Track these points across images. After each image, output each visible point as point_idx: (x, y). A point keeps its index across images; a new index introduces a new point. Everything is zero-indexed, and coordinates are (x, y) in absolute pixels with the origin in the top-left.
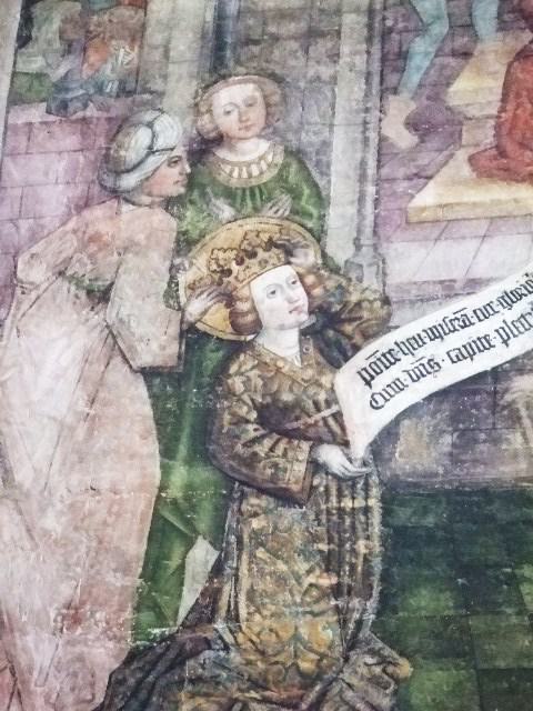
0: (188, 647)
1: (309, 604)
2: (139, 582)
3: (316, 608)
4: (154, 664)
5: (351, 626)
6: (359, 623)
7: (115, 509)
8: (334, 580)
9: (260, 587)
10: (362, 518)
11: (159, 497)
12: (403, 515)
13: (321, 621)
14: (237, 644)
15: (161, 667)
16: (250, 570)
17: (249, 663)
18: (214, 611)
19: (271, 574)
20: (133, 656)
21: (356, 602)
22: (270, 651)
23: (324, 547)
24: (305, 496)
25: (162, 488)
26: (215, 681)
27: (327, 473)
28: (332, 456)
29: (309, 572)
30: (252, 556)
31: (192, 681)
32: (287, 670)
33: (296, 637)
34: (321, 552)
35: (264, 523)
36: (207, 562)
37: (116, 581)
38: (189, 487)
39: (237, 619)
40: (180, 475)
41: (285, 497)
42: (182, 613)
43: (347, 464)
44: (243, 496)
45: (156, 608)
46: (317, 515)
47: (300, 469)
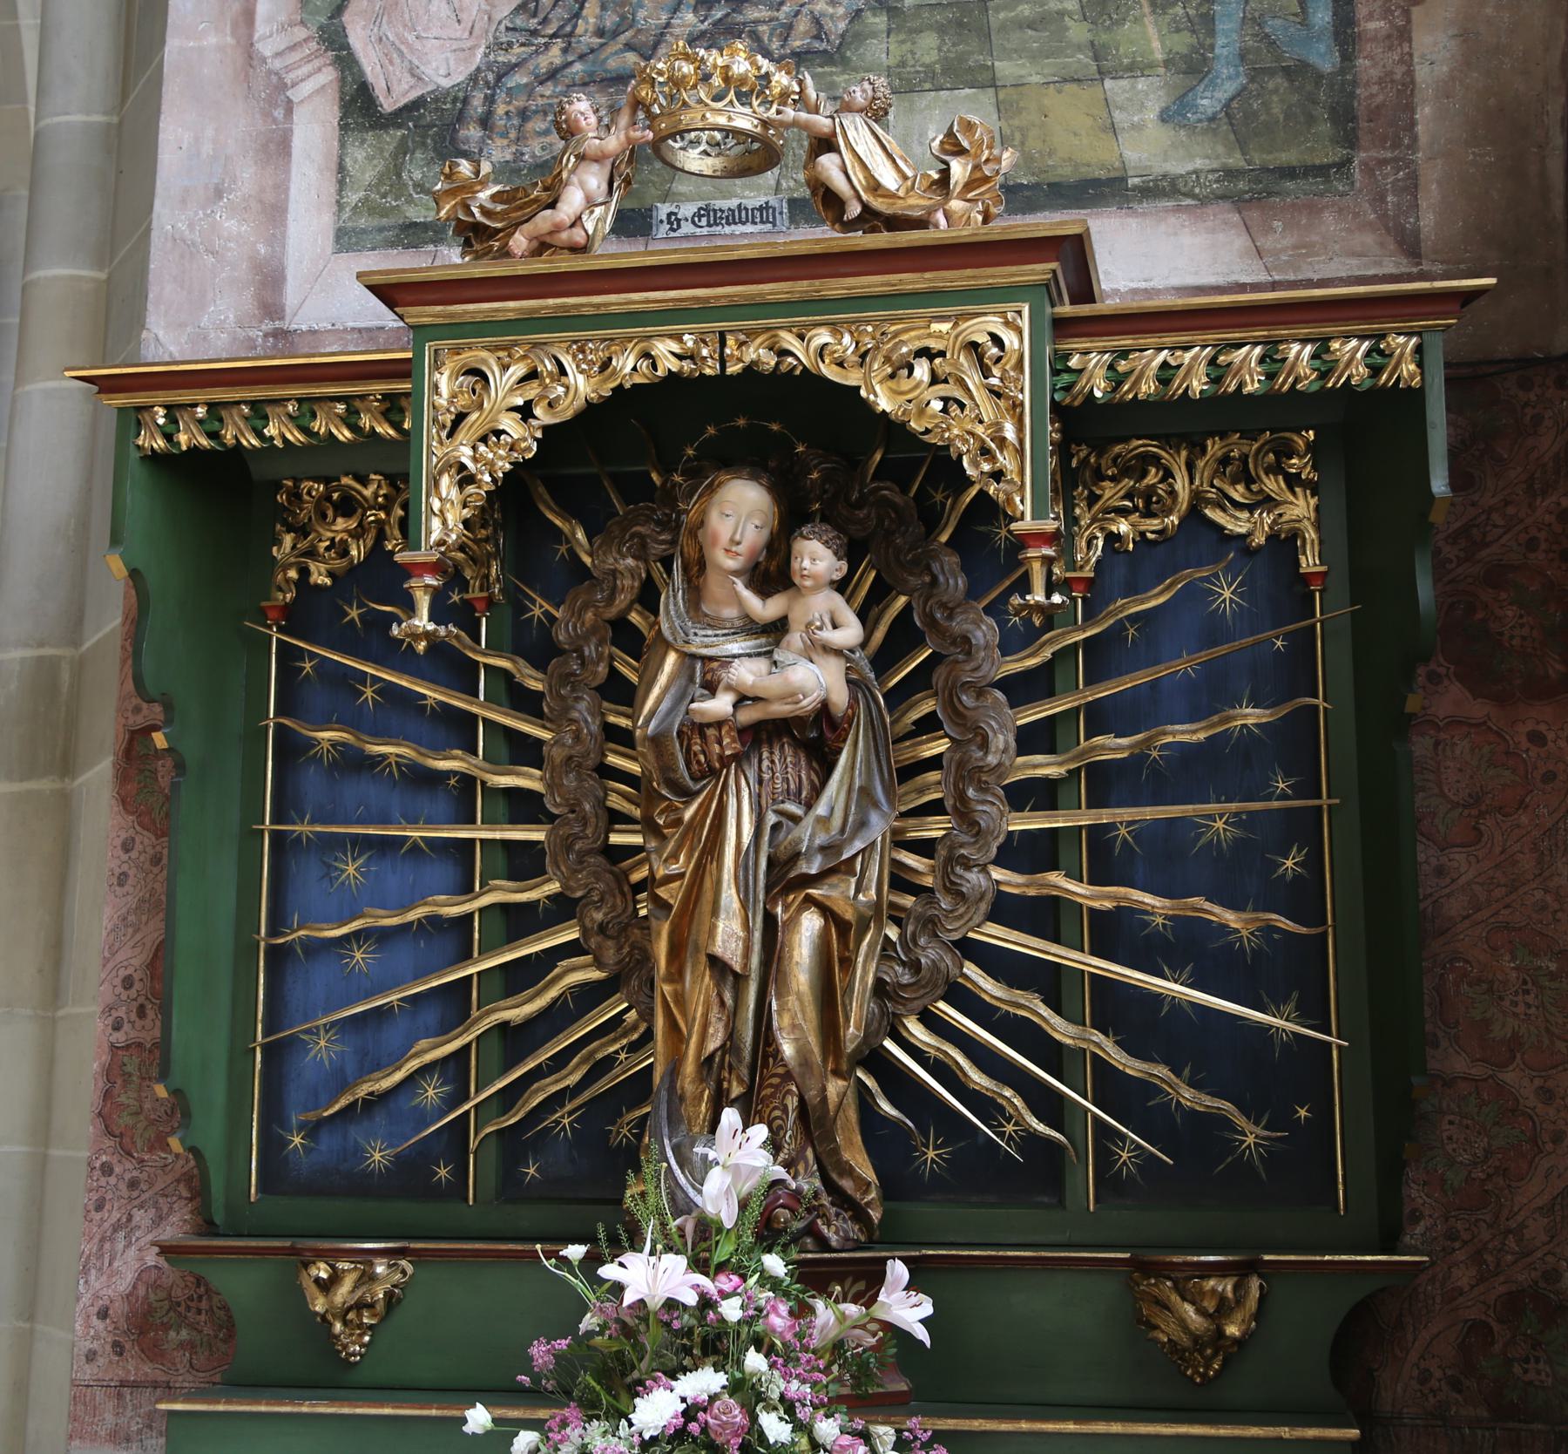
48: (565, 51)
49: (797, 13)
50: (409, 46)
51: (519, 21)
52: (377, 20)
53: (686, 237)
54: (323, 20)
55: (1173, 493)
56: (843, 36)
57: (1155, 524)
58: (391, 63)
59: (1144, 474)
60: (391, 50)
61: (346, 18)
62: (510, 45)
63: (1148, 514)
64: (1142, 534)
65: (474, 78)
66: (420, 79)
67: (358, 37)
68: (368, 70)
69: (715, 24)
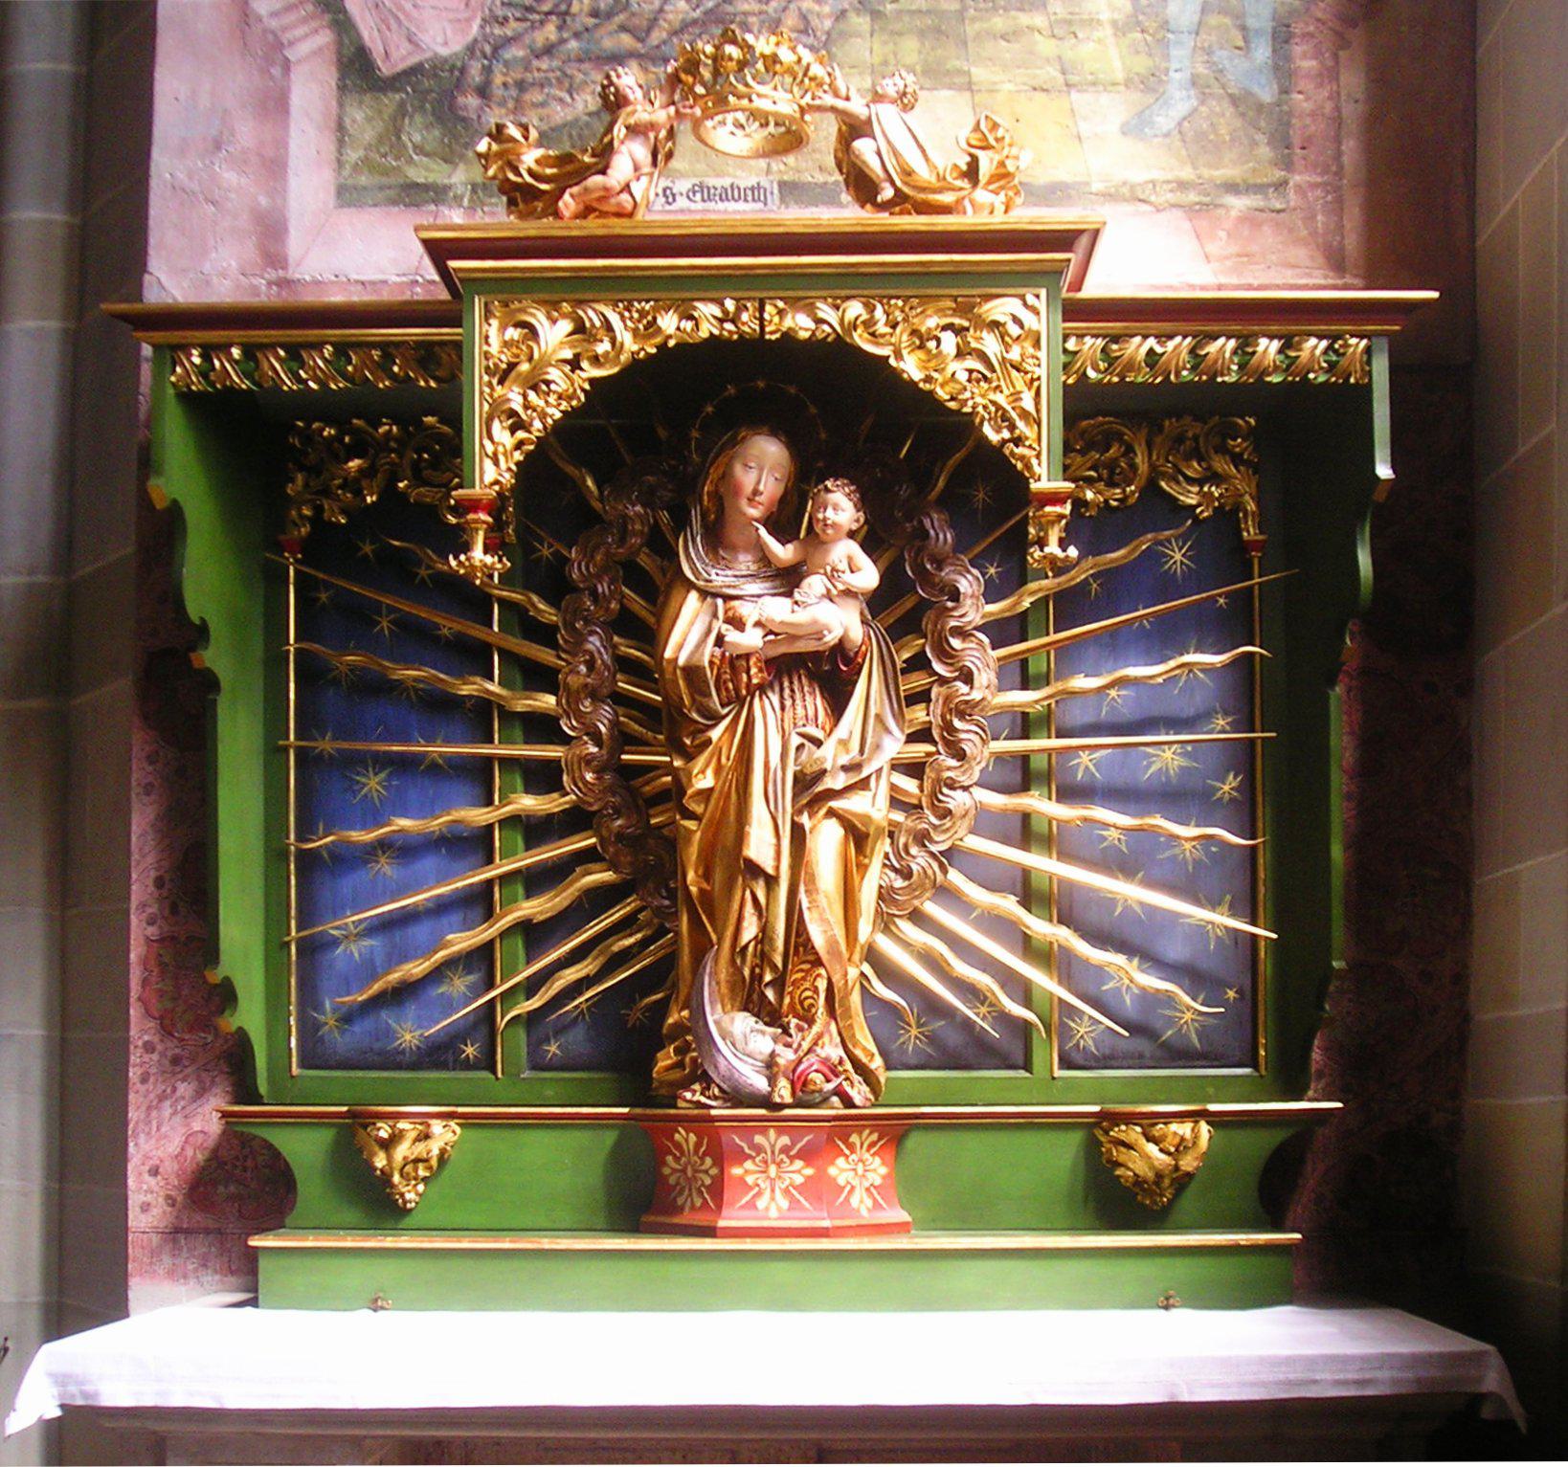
48: (560, 28)
49: (785, 9)
50: (407, 15)
53: (682, 211)
58: (389, 29)
60: (388, 18)
62: (506, 19)
65: (471, 49)
66: (417, 45)
68: (365, 34)
69: (706, 13)
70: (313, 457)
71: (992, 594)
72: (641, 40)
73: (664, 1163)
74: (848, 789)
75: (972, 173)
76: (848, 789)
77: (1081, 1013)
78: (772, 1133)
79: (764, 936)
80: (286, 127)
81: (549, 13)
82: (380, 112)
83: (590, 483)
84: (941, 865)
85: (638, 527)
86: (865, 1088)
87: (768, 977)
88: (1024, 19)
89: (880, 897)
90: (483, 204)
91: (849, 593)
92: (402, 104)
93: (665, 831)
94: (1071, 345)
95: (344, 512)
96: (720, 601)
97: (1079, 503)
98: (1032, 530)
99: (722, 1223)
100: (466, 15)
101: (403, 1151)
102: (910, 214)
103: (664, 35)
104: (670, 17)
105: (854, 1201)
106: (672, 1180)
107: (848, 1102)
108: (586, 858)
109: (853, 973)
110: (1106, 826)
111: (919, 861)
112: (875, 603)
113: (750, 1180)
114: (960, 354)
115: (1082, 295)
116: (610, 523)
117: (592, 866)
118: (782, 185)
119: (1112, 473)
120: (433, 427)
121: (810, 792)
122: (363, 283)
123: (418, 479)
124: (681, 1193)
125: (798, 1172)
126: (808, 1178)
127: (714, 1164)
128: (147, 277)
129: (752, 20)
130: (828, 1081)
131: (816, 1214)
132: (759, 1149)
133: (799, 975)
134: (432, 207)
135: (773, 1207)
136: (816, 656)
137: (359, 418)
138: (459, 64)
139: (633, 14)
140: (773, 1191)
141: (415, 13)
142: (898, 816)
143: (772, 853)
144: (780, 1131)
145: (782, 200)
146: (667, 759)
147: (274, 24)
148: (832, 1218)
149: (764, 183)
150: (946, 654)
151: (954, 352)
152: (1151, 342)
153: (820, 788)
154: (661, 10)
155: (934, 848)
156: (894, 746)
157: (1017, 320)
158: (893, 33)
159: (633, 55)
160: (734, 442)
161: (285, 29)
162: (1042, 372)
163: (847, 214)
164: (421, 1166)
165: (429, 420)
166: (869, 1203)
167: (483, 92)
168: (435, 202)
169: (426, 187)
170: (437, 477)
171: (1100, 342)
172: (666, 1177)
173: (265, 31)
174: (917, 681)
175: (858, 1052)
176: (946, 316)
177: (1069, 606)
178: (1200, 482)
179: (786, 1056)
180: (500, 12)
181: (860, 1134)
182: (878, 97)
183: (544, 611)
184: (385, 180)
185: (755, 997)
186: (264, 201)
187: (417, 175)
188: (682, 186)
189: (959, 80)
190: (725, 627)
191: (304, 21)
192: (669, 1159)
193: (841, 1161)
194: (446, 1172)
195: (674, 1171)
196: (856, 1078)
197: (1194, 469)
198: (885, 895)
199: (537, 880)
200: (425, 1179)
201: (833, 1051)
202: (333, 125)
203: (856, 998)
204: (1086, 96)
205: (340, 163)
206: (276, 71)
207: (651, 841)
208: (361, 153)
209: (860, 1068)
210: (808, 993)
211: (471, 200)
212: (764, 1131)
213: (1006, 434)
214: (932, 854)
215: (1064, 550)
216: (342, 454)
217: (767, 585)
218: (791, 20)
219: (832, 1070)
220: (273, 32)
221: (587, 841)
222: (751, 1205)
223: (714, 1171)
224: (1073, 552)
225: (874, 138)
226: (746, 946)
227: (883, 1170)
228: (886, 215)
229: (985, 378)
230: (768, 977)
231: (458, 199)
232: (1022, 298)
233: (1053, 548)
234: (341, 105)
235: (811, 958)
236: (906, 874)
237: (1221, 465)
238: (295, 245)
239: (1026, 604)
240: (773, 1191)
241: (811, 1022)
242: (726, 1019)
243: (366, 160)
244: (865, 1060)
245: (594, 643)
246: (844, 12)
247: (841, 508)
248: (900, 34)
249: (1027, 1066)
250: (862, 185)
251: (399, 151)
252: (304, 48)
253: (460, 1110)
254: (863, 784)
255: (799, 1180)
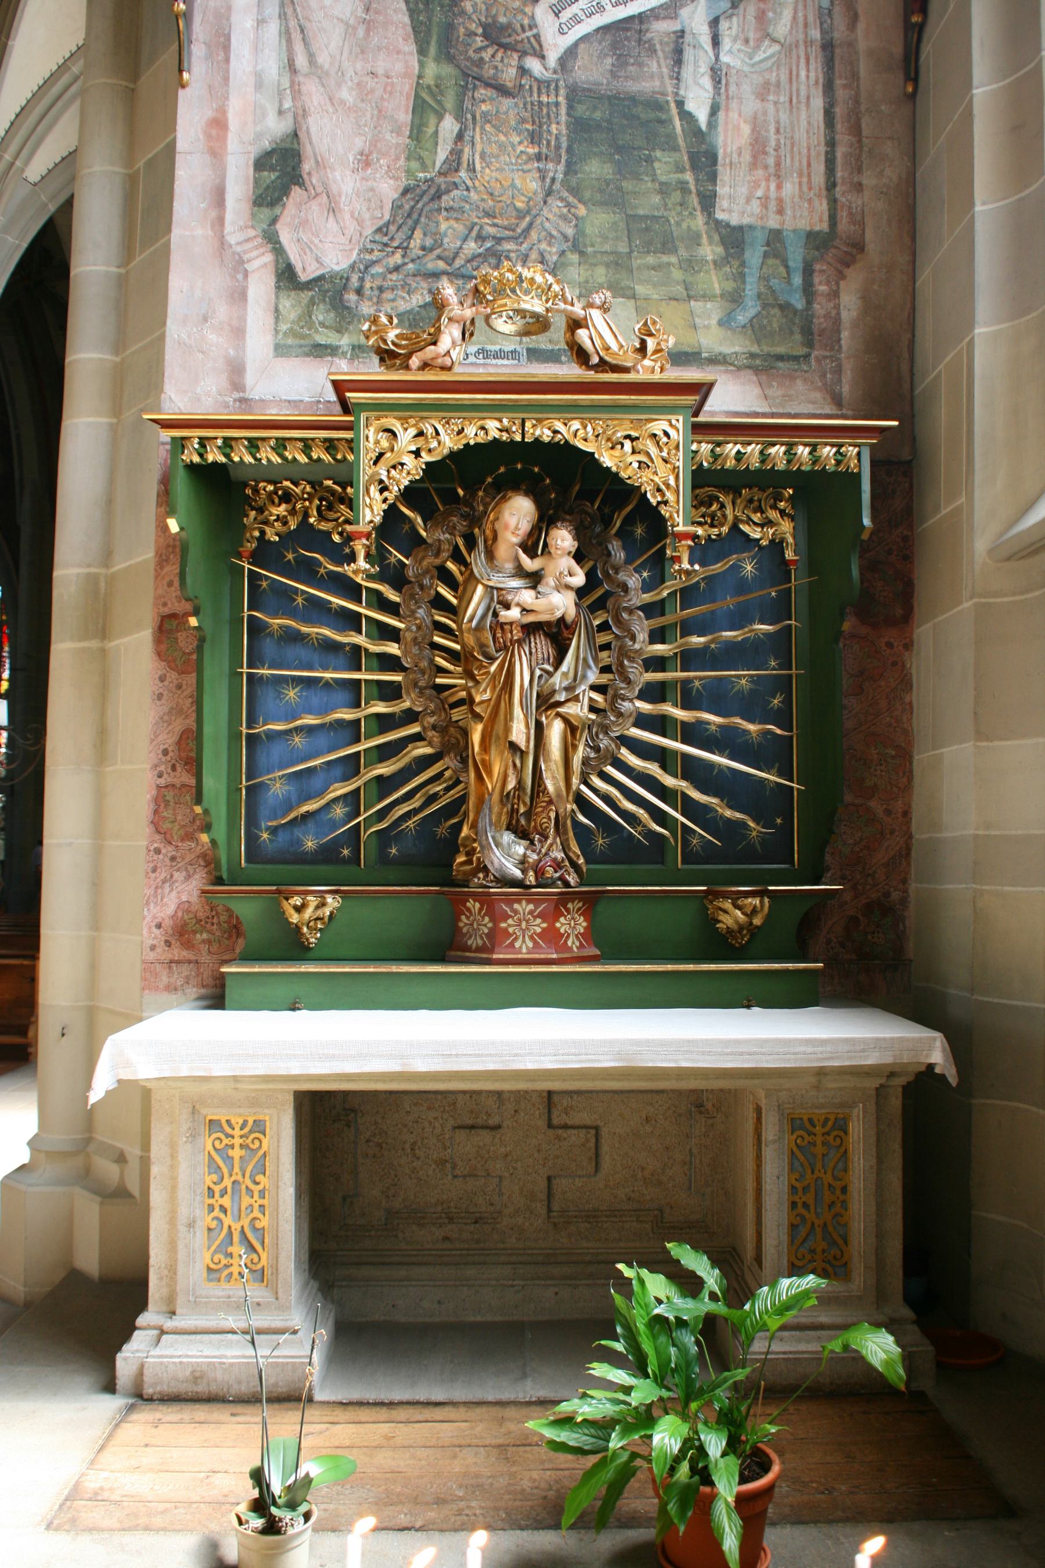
0: (443, 187)
1: (520, 165)
2: (408, 141)
3: (525, 167)
4: (421, 196)
5: (548, 180)
6: (553, 180)
7: (389, 88)
8: (536, 150)
9: (488, 151)
10: (554, 109)
11: (418, 83)
12: (581, 110)
13: (529, 176)
14: (475, 187)
15: (425, 199)
16: (481, 138)
17: (483, 200)
18: (459, 164)
19: (495, 142)
20: (406, 191)
21: (550, 166)
22: (496, 193)
23: (529, 127)
24: (516, 91)
25: (420, 77)
26: (461, 210)
27: (531, 76)
28: (533, 65)
29: (520, 143)
30: (482, 128)
31: (446, 209)
32: (507, 206)
33: (513, 186)
34: (527, 130)
35: (489, 107)
36: (452, 131)
37: (392, 139)
38: (438, 77)
39: (474, 171)
40: (432, 69)
41: (503, 91)
42: (438, 164)
43: (544, 71)
44: (475, 88)
45: (420, 158)
46: (525, 105)
47: (513, 72)
48: (403, 256)
49: (531, 249)
50: (315, 245)
51: (377, 238)
52: (296, 229)
53: (472, 364)
54: (265, 226)
55: (724, 516)
56: (555, 264)
57: (716, 531)
58: (305, 253)
59: (711, 505)
60: (305, 248)
61: (278, 226)
62: (372, 250)
63: (712, 526)
64: (709, 536)
65: (352, 267)
66: (322, 264)
67: (286, 237)
69: (486, 250)
70: (260, 503)
71: (647, 587)
72: (450, 265)
73: (460, 920)
74: (567, 701)
75: (642, 349)
76: (567, 701)
77: (694, 831)
78: (524, 903)
79: (520, 785)
80: (245, 309)
81: (396, 248)
82: (300, 302)
83: (419, 520)
84: (616, 745)
85: (447, 547)
86: (575, 876)
87: (522, 810)
88: (665, 259)
89: (583, 763)
90: (358, 357)
91: (568, 587)
92: (312, 298)
93: (460, 723)
94: (694, 447)
95: (277, 534)
96: (495, 592)
97: (695, 537)
98: (668, 552)
99: (495, 956)
100: (349, 247)
101: (308, 913)
102: (607, 372)
103: (463, 262)
104: (466, 251)
105: (569, 943)
106: (465, 930)
107: (567, 884)
108: (417, 738)
109: (569, 807)
110: (709, 723)
111: (604, 742)
112: (581, 593)
113: (511, 930)
114: (634, 452)
115: (701, 418)
116: (431, 545)
117: (418, 744)
118: (529, 350)
119: (713, 519)
120: (328, 486)
121: (546, 702)
122: (289, 402)
123: (321, 517)
124: (470, 937)
125: (538, 925)
126: (544, 929)
127: (490, 921)
128: (163, 396)
129: (512, 255)
130: (556, 872)
131: (549, 950)
132: (516, 912)
133: (540, 809)
134: (329, 358)
135: (524, 946)
136: (548, 624)
137: (286, 480)
138: (345, 275)
139: (445, 249)
140: (524, 937)
141: (320, 245)
142: (593, 716)
143: (524, 739)
144: (529, 902)
145: (529, 359)
146: (463, 681)
147: (239, 249)
148: (557, 952)
149: (518, 349)
150: (619, 621)
151: (630, 451)
152: (738, 447)
153: (552, 701)
154: (461, 248)
155: (613, 735)
156: (593, 676)
157: (666, 434)
158: (592, 265)
159: (444, 273)
160: (505, 499)
161: (245, 252)
162: (680, 464)
163: (570, 371)
164: (319, 922)
165: (329, 483)
166: (578, 944)
167: (359, 292)
168: (331, 355)
169: (326, 347)
170: (332, 515)
171: (710, 446)
172: (461, 929)
173: (234, 253)
174: (602, 638)
175: (571, 854)
176: (626, 430)
177: (688, 595)
178: (762, 526)
179: (533, 857)
180: (369, 246)
181: (573, 903)
182: (591, 305)
183: (393, 596)
184: (302, 342)
185: (514, 822)
186: (232, 352)
187: (321, 339)
188: (472, 349)
189: (629, 293)
190: (498, 606)
191: (256, 248)
192: (463, 917)
193: (562, 919)
194: (334, 924)
195: (466, 924)
196: (571, 870)
197: (757, 517)
198: (585, 762)
199: (385, 752)
200: (320, 930)
201: (559, 855)
202: (273, 309)
203: (569, 822)
204: (700, 304)
205: (277, 331)
206: (240, 277)
207: (452, 729)
208: (289, 325)
209: (574, 865)
210: (545, 820)
211: (352, 355)
212: (519, 901)
213: (659, 499)
214: (611, 739)
215: (692, 566)
216: (277, 501)
217: (522, 582)
218: (534, 255)
219: (557, 865)
220: (238, 254)
221: (415, 729)
222: (512, 945)
223: (490, 925)
224: (697, 567)
225: (588, 329)
226: (508, 793)
227: (585, 924)
228: (593, 372)
229: (648, 467)
230: (522, 810)
231: (344, 354)
232: (670, 421)
233: (686, 565)
234: (277, 297)
235: (546, 799)
236: (597, 749)
237: (773, 515)
238: (249, 379)
239: (665, 594)
240: (524, 937)
241: (546, 838)
242: (498, 835)
243: (291, 329)
244: (575, 859)
245: (421, 612)
246: (563, 252)
247: (563, 539)
248: (595, 265)
249: (662, 863)
250: (581, 355)
251: (310, 325)
252: (257, 263)
253: (342, 888)
254: (576, 699)
255: (539, 930)
